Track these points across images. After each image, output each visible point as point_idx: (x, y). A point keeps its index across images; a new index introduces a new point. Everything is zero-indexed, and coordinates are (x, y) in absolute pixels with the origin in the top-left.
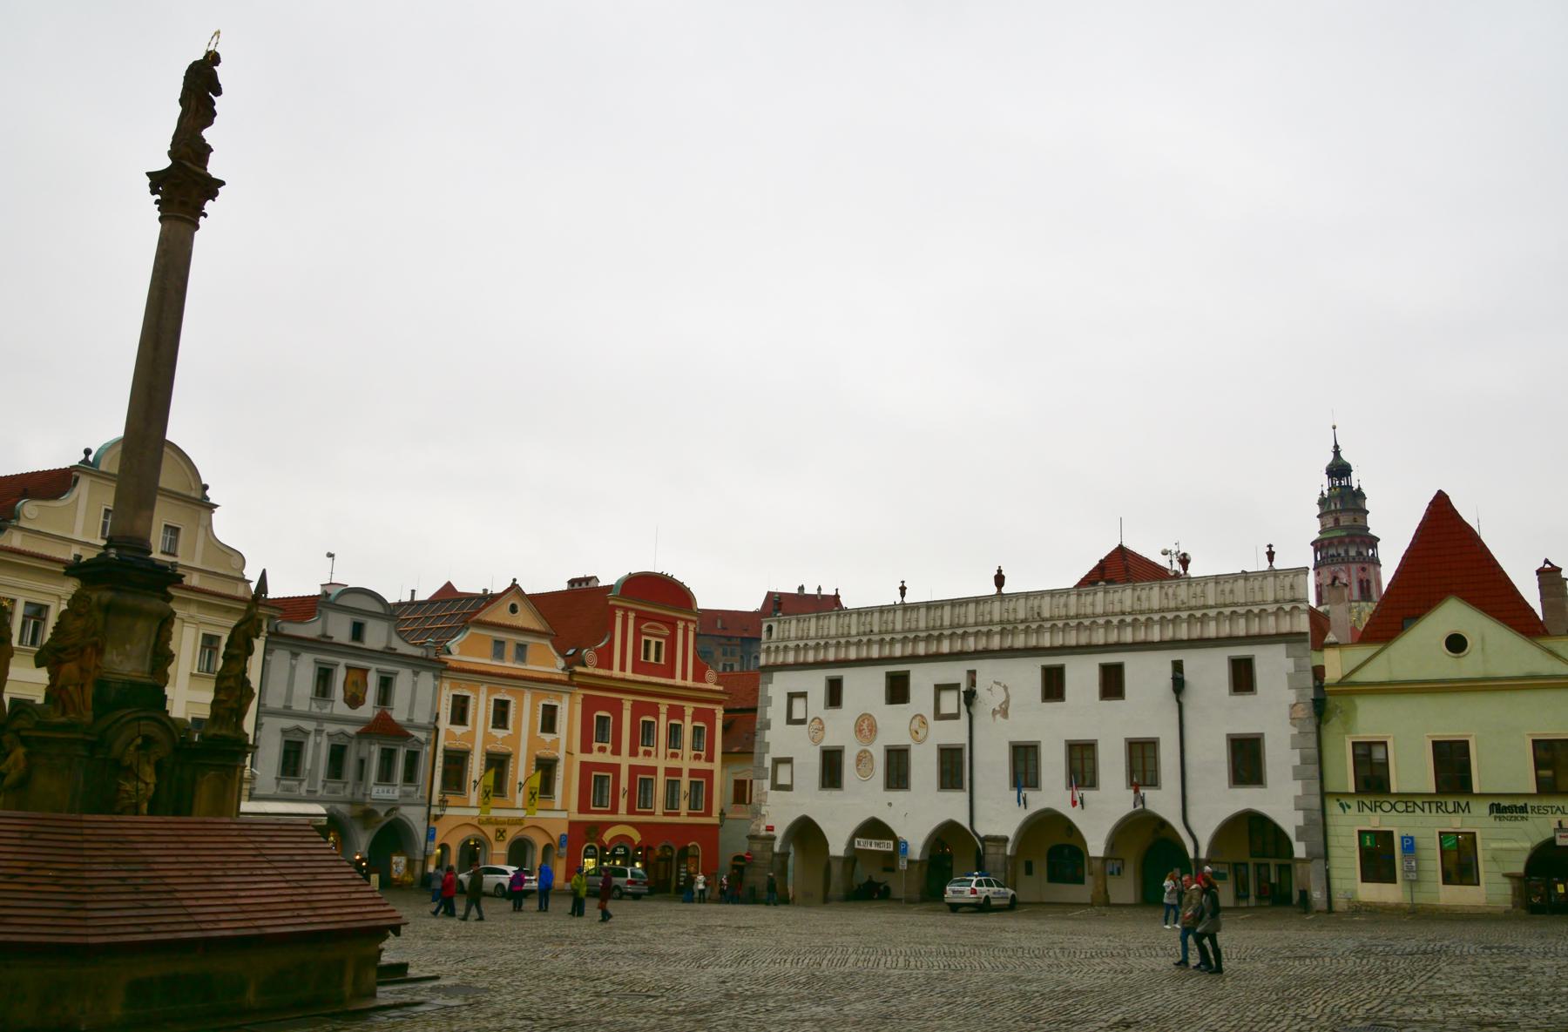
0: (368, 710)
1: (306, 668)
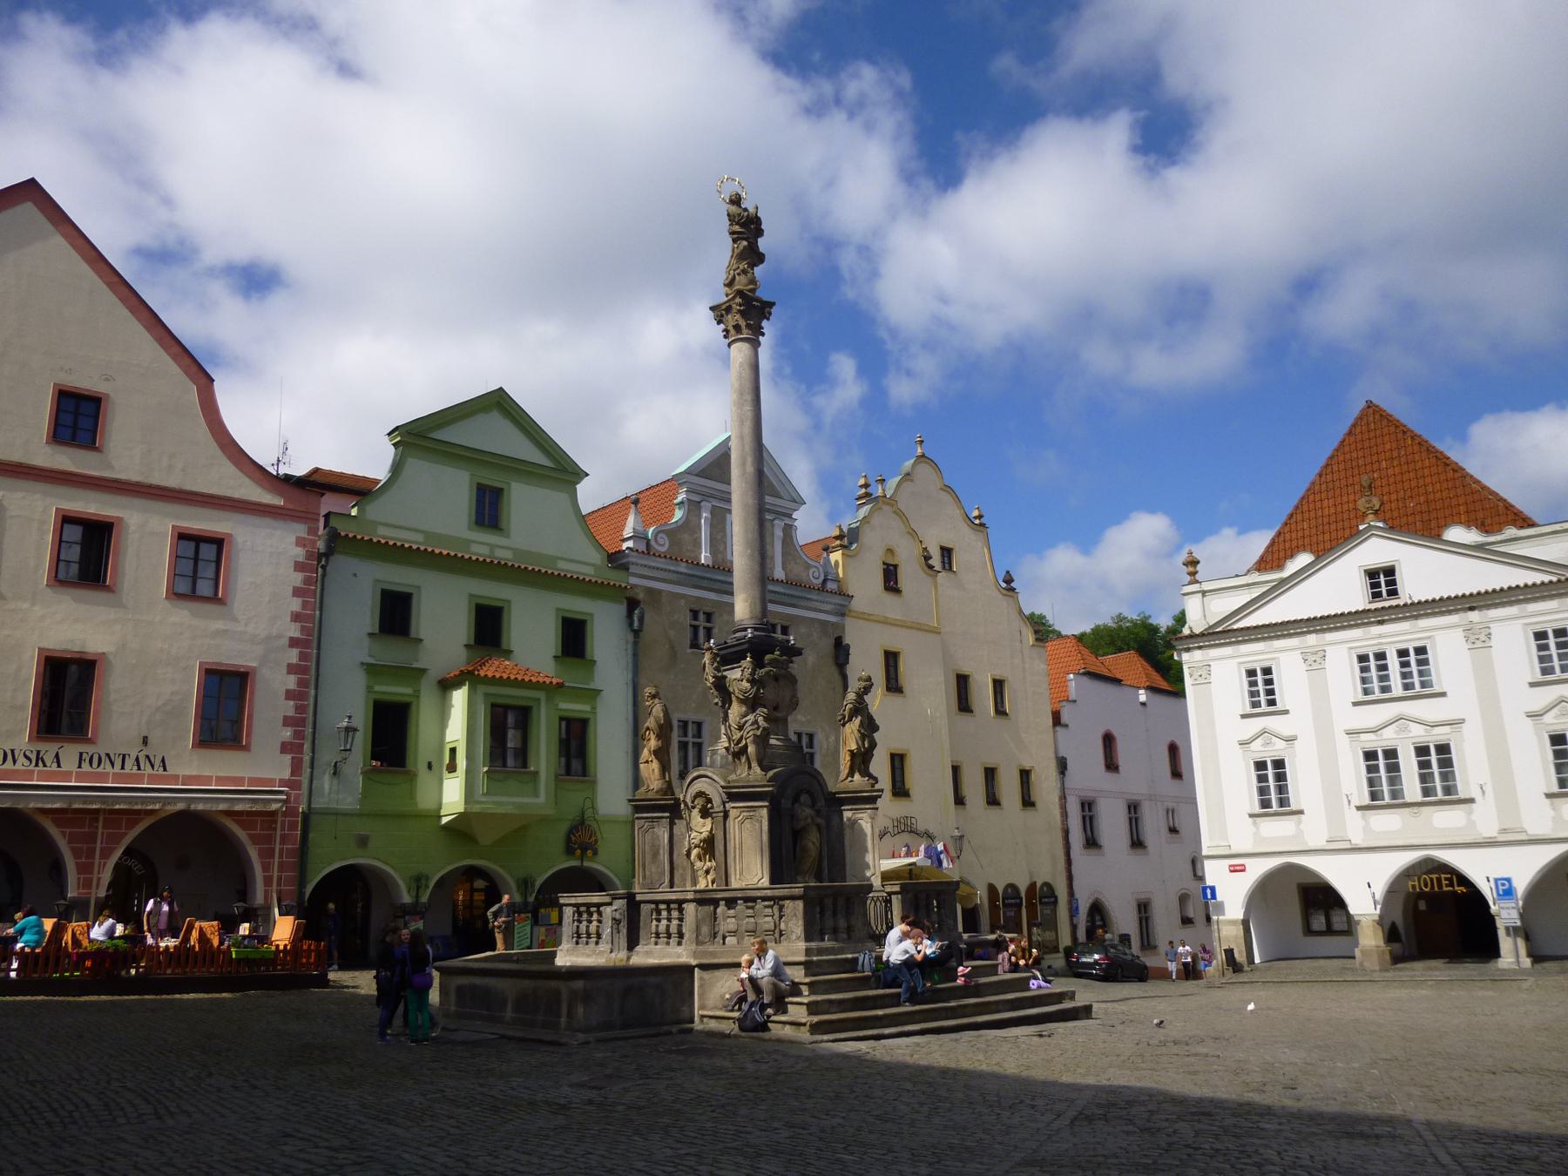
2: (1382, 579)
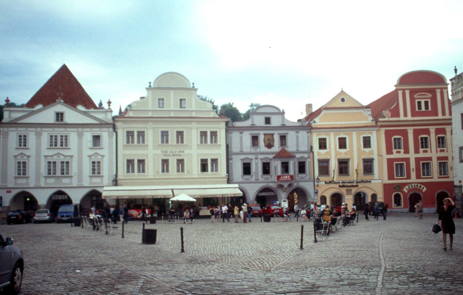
0: (277, 148)
1: (247, 137)
2: (60, 116)
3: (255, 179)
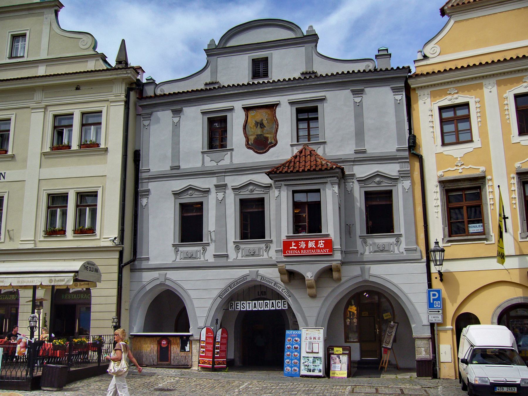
1: (193, 123)
3: (215, 256)
